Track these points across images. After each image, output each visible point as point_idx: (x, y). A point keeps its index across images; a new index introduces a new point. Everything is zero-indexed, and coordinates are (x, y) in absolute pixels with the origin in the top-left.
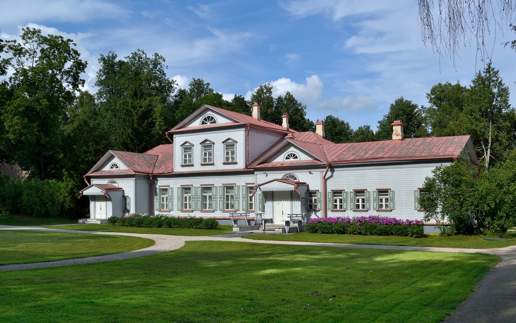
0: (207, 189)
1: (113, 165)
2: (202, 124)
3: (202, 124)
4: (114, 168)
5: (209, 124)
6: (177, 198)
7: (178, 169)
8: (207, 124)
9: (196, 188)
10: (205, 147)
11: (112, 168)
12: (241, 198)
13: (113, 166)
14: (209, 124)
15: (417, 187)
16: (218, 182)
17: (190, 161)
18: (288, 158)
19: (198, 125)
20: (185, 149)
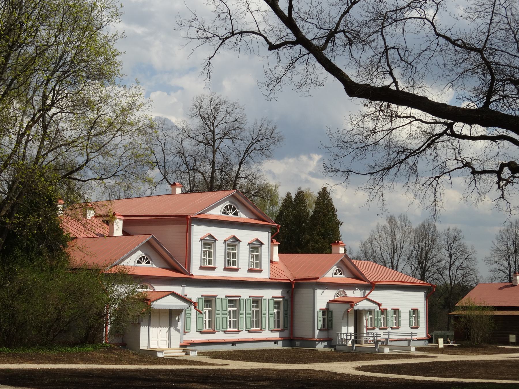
0: (233, 301)
1: (140, 258)
2: (224, 213)
3: (224, 213)
4: (144, 264)
5: (230, 215)
6: (192, 314)
7: (196, 272)
8: (228, 214)
9: (222, 300)
10: (229, 245)
11: (139, 262)
12: (267, 314)
13: (141, 260)
14: (230, 215)
15: (411, 308)
16: (245, 294)
17: (234, 263)
18: (336, 274)
19: (219, 214)
20: (204, 244)
